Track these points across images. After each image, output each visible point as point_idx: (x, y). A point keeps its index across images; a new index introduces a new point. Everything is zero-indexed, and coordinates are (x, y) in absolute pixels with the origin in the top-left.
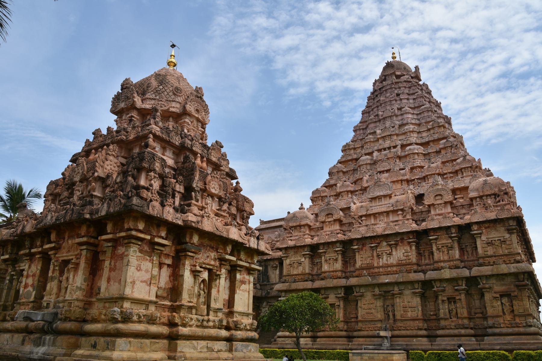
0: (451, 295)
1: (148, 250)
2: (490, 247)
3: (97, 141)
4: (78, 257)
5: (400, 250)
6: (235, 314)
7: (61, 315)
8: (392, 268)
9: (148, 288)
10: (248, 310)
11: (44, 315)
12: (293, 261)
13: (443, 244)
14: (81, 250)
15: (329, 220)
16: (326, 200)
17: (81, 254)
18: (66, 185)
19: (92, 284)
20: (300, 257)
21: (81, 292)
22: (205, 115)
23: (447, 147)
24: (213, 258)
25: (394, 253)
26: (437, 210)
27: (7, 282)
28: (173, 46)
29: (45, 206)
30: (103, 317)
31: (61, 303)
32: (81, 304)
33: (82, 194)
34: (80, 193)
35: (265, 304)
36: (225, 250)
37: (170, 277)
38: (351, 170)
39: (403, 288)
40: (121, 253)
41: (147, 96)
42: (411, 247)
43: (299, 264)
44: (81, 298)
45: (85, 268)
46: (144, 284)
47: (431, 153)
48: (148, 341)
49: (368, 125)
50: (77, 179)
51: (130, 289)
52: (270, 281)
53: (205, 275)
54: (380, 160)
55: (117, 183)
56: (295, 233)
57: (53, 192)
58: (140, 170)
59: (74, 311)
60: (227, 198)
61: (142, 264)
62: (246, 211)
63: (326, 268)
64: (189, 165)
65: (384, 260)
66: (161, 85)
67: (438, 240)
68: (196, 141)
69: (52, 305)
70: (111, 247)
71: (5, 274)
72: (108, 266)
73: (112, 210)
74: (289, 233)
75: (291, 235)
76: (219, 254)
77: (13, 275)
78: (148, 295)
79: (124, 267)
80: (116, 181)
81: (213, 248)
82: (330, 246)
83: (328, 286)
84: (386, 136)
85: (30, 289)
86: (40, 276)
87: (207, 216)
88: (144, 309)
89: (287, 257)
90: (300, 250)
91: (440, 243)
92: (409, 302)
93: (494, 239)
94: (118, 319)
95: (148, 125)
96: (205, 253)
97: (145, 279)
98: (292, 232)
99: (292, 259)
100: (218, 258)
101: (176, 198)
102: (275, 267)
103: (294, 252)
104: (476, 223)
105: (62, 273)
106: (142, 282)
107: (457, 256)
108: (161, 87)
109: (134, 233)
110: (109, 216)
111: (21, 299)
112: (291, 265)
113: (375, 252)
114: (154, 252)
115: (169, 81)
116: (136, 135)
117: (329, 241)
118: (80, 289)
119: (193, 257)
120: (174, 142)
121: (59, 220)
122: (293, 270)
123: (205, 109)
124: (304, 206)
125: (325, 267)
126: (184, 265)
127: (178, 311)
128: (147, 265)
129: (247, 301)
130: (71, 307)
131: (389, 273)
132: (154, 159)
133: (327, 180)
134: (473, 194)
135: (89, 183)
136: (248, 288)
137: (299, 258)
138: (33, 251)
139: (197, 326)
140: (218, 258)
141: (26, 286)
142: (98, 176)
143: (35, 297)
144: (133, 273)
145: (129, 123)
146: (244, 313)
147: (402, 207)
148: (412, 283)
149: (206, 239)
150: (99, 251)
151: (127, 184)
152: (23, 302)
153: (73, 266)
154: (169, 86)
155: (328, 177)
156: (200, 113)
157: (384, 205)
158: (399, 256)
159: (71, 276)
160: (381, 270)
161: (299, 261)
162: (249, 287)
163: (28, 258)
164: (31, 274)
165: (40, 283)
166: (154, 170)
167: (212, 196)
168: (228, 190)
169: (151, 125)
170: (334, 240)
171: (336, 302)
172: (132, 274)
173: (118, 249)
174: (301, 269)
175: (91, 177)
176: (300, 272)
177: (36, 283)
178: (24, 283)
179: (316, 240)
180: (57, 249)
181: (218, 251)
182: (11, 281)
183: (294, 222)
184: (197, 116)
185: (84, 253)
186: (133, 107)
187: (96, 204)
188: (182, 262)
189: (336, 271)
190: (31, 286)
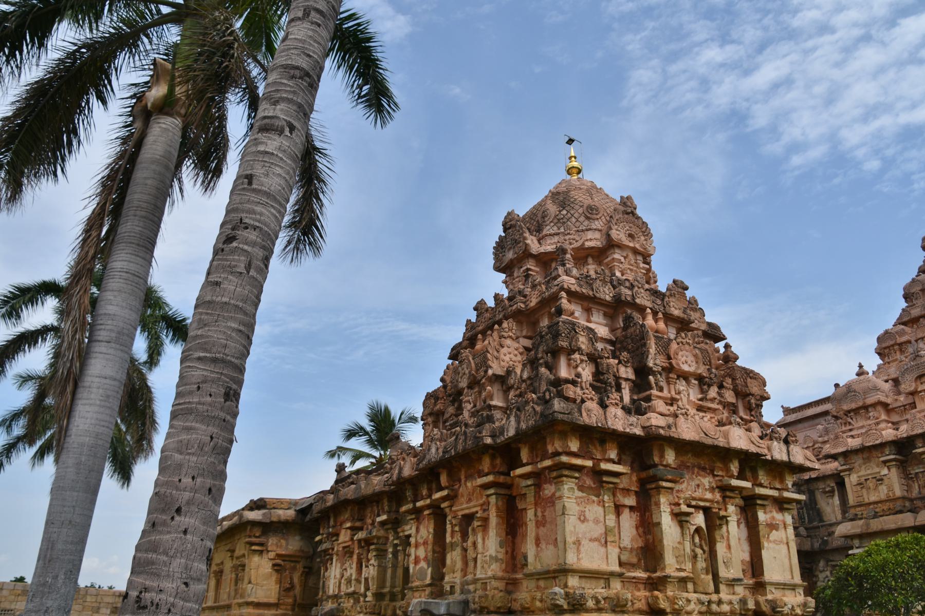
3: (483, 320)
4: (484, 507)
6: (768, 588)
7: (474, 604)
9: (603, 550)
10: (793, 578)
11: (448, 605)
12: (864, 476)
14: (488, 496)
16: (911, 350)
17: (489, 503)
18: (450, 396)
19: (513, 551)
20: (878, 466)
21: (498, 564)
22: (646, 240)
24: (707, 487)
27: (390, 556)
28: (570, 141)
29: (425, 434)
30: (538, 604)
31: (471, 584)
32: (501, 585)
33: (475, 406)
34: (472, 405)
35: (822, 564)
36: (728, 470)
37: (637, 528)
40: (550, 494)
41: (545, 232)
43: (878, 480)
44: (500, 574)
45: (498, 524)
46: (596, 543)
50: (463, 384)
51: (574, 553)
52: (825, 519)
53: (699, 519)
55: (524, 381)
56: (858, 422)
57: (433, 409)
58: (555, 353)
59: (493, 597)
60: (712, 376)
62: (753, 395)
64: (635, 331)
66: (564, 208)
68: (639, 288)
69: (458, 589)
70: (533, 487)
71: (386, 544)
72: (533, 518)
73: (523, 426)
74: (845, 424)
75: (851, 427)
76: (717, 478)
77: (396, 545)
78: (605, 562)
79: (558, 518)
80: (521, 377)
81: (704, 469)
85: (423, 564)
86: (434, 543)
87: (683, 415)
88: (603, 588)
89: (850, 470)
90: (874, 453)
94: (562, 606)
95: (555, 278)
96: (693, 479)
98: (850, 420)
99: (862, 473)
100: (717, 487)
101: (623, 391)
102: (829, 492)
103: (863, 459)
105: (465, 536)
106: (591, 540)
108: (564, 212)
109: (564, 459)
110: (521, 437)
111: (412, 582)
112: (861, 484)
114: (603, 487)
115: (576, 200)
116: (539, 299)
118: (496, 559)
119: (671, 489)
120: (602, 297)
121: (447, 452)
122: (868, 493)
123: (644, 229)
124: (865, 368)
126: (658, 504)
127: (662, 588)
128: (594, 511)
129: (786, 561)
130: (486, 589)
132: (576, 332)
133: (903, 310)
135: (482, 388)
136: (784, 536)
137: (877, 470)
138: (419, 504)
140: (717, 487)
141: (417, 561)
142: (494, 375)
143: (432, 578)
144: (575, 527)
145: (525, 281)
146: (785, 585)
149: (690, 455)
150: (514, 494)
151: (540, 379)
152: (417, 587)
153: (479, 523)
154: (577, 207)
155: (904, 304)
156: (637, 239)
159: (480, 540)
162: (786, 534)
163: (413, 516)
164: (421, 541)
165: (436, 555)
166: (579, 350)
167: (685, 376)
168: (713, 361)
169: (560, 276)
172: (572, 529)
173: (544, 489)
175: (483, 377)
176: (883, 497)
177: (430, 554)
178: (413, 557)
179: (904, 430)
180: (452, 498)
181: (715, 473)
182: (395, 554)
183: (852, 401)
184: (631, 245)
185: (493, 500)
186: (527, 254)
187: (498, 420)
188: (653, 500)
190: (423, 559)
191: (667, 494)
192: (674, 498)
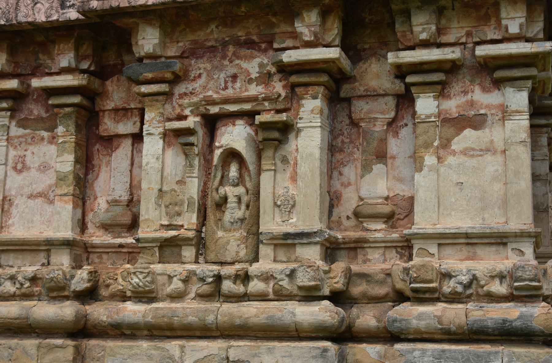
1: (44, 115)
46: (39, 200)
48: (30, 344)
61: (28, 153)
81: (250, 44)
96: (221, 68)
97: (40, 190)
106: (31, 197)
139: (202, 297)
146: (467, 236)
181: (276, 46)
191: (159, 105)
192: (174, 107)
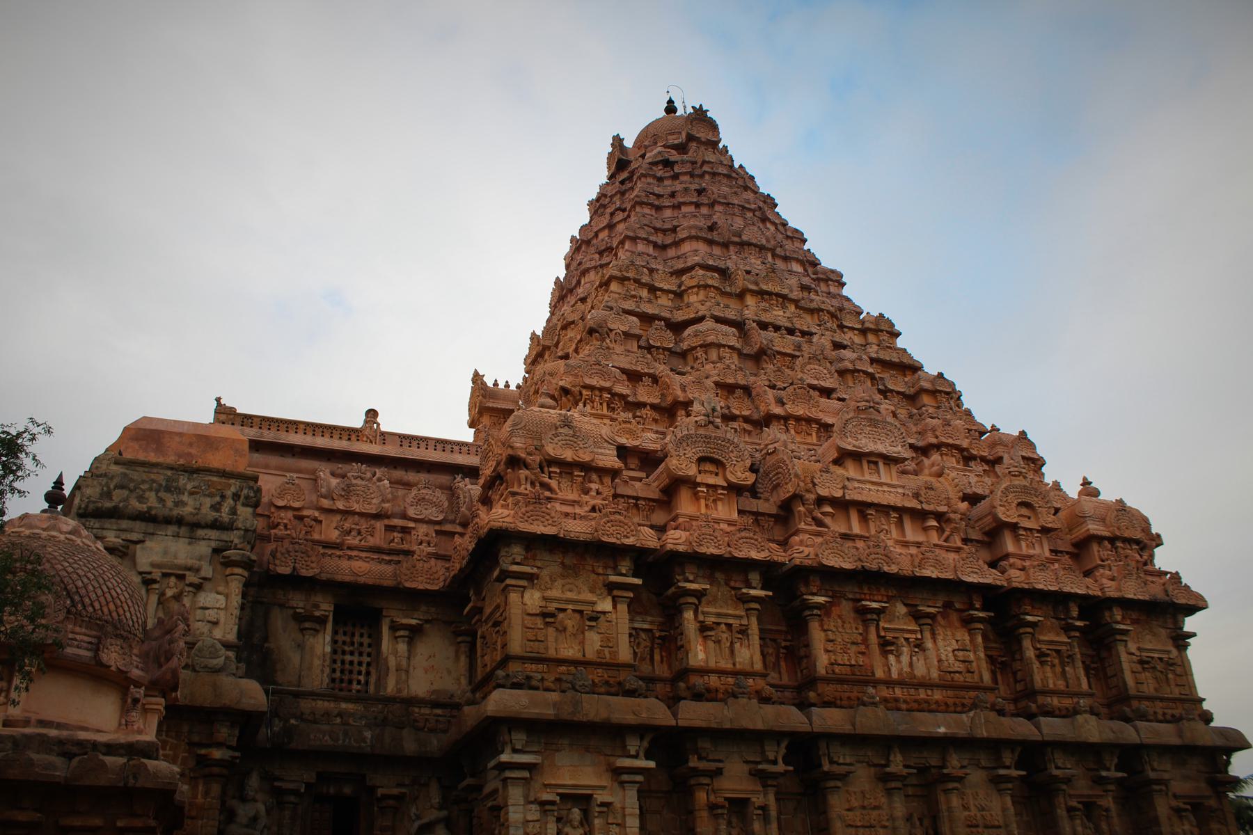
0: (1089, 796)
2: (1147, 674)
5: (944, 640)
8: (929, 692)
13: (1051, 642)
15: (711, 480)
20: (592, 591)
23: (940, 392)
25: (929, 644)
26: (1023, 544)
38: (665, 349)
39: (965, 763)
42: (971, 632)
43: (591, 619)
47: (892, 391)
49: (683, 240)
54: (779, 353)
63: (701, 656)
65: (898, 665)
67: (1037, 629)
74: (533, 484)
82: (720, 576)
83: (747, 724)
84: (770, 293)
89: (531, 578)
91: (1046, 638)
92: (983, 809)
93: (1152, 655)
103: (562, 563)
104: (1126, 604)
107: (1085, 686)
112: (553, 615)
113: (873, 629)
117: (737, 554)
125: (699, 654)
131: (925, 705)
134: (1095, 527)
137: (590, 597)
147: (943, 509)
148: (994, 746)
157: (888, 485)
158: (943, 657)
160: (898, 692)
161: (587, 609)
170: (754, 555)
171: (753, 792)
174: (594, 641)
176: (591, 655)
183: (568, 445)
189: (747, 674)
